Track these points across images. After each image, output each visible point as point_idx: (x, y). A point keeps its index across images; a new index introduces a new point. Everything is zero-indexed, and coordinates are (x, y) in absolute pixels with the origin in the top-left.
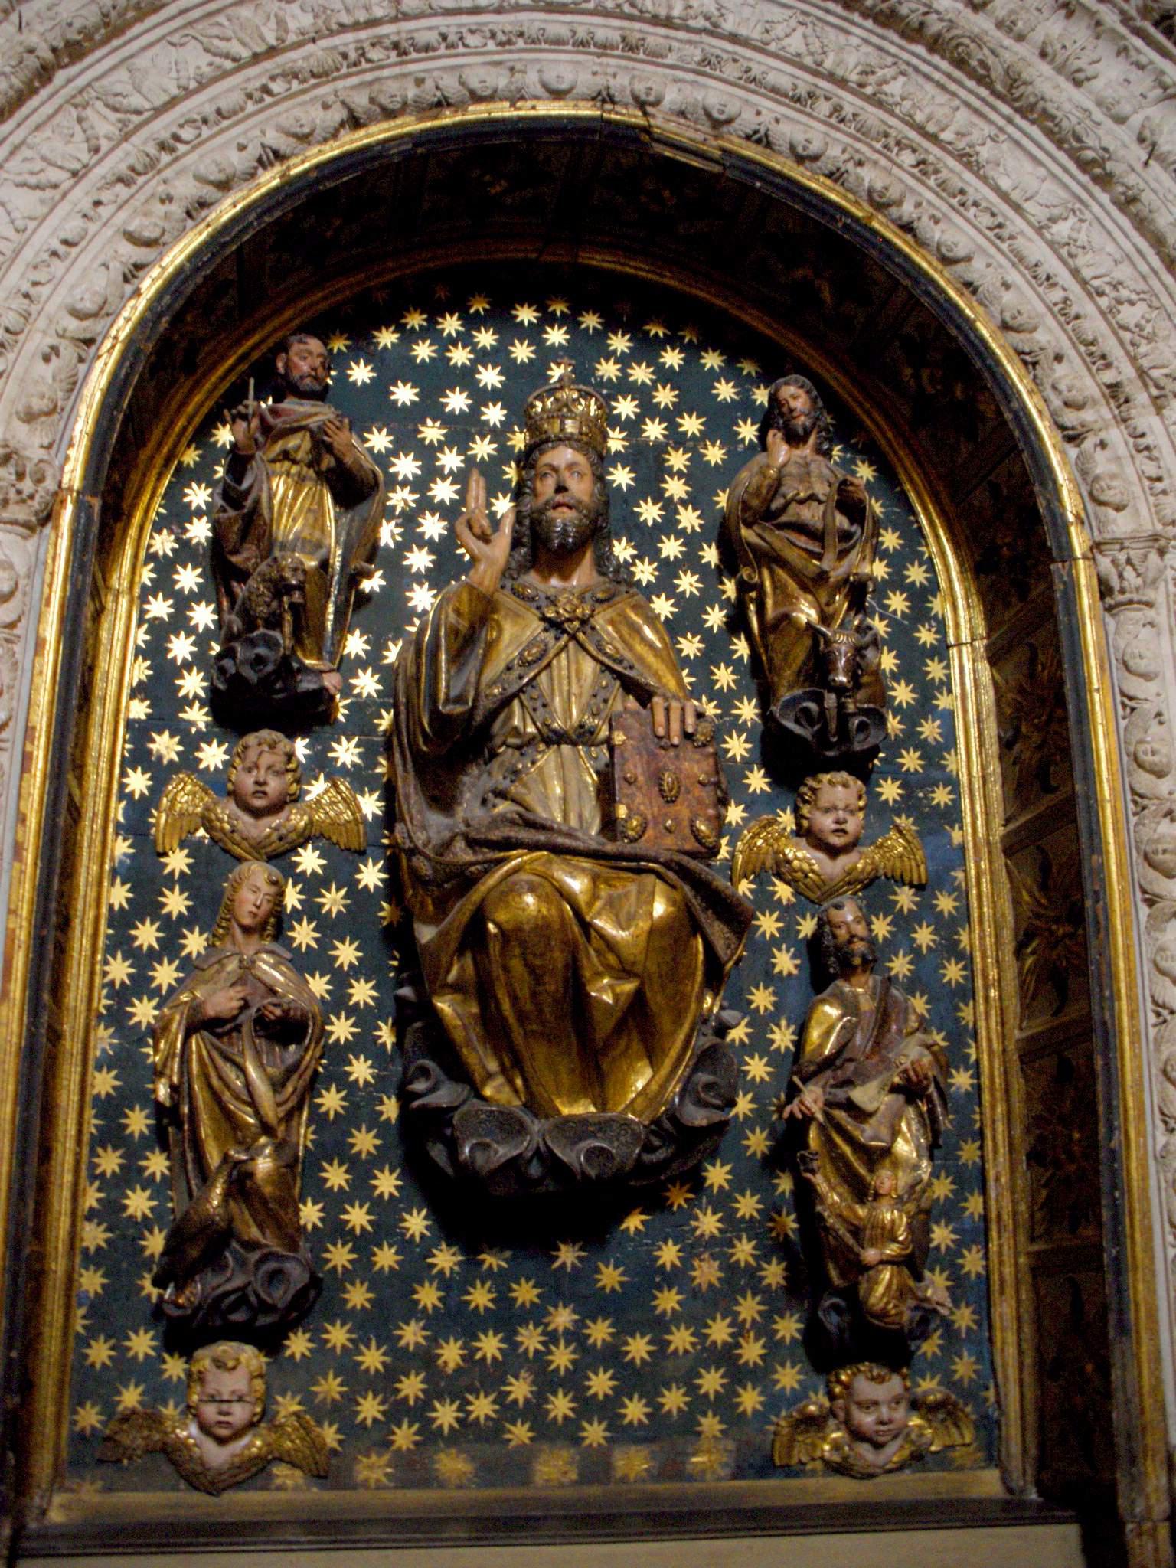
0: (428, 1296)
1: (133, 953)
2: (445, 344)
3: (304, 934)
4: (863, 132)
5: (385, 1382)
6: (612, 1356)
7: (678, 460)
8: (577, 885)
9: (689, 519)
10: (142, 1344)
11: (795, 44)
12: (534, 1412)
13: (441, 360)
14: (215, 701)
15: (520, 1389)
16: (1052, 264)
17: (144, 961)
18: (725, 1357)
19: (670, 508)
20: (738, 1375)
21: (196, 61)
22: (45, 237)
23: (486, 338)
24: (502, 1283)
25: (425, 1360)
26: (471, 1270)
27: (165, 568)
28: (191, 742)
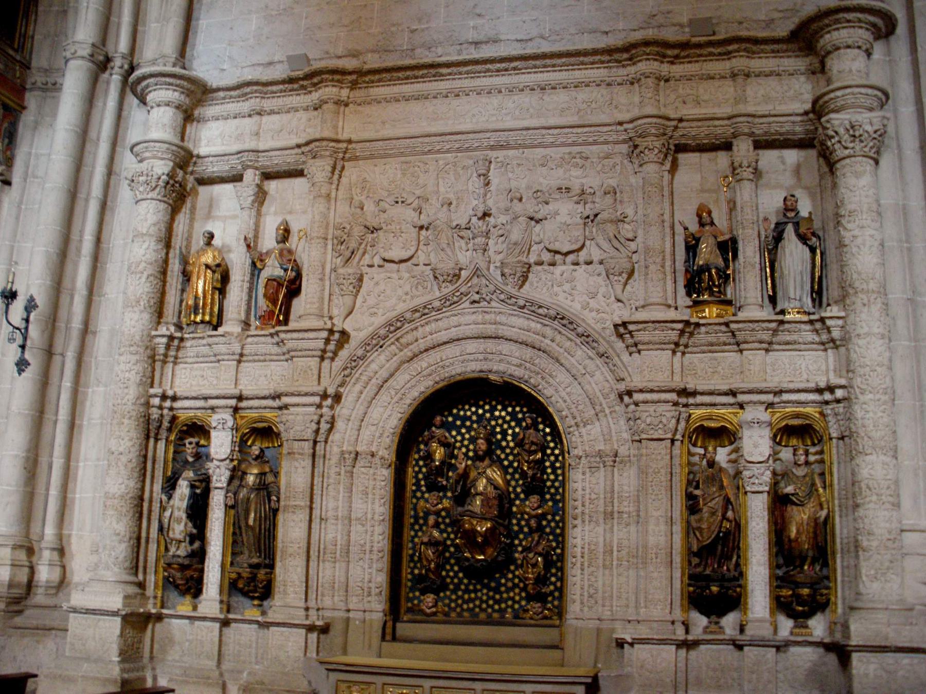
0: (463, 587)
1: (414, 530)
2: (465, 411)
3: (442, 526)
4: (531, 372)
5: (455, 601)
6: (493, 598)
7: (510, 432)
8: (475, 523)
9: (512, 444)
10: (417, 594)
11: (517, 354)
12: (480, 607)
13: (465, 415)
14: (426, 486)
15: (477, 603)
16: (567, 398)
17: (416, 531)
18: (512, 599)
19: (508, 442)
20: (515, 602)
21: (408, 377)
22: (385, 416)
23: (473, 409)
24: (475, 585)
25: (462, 597)
26: (470, 583)
27: (417, 461)
28: (423, 493)
